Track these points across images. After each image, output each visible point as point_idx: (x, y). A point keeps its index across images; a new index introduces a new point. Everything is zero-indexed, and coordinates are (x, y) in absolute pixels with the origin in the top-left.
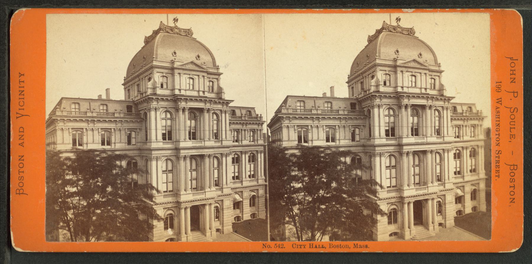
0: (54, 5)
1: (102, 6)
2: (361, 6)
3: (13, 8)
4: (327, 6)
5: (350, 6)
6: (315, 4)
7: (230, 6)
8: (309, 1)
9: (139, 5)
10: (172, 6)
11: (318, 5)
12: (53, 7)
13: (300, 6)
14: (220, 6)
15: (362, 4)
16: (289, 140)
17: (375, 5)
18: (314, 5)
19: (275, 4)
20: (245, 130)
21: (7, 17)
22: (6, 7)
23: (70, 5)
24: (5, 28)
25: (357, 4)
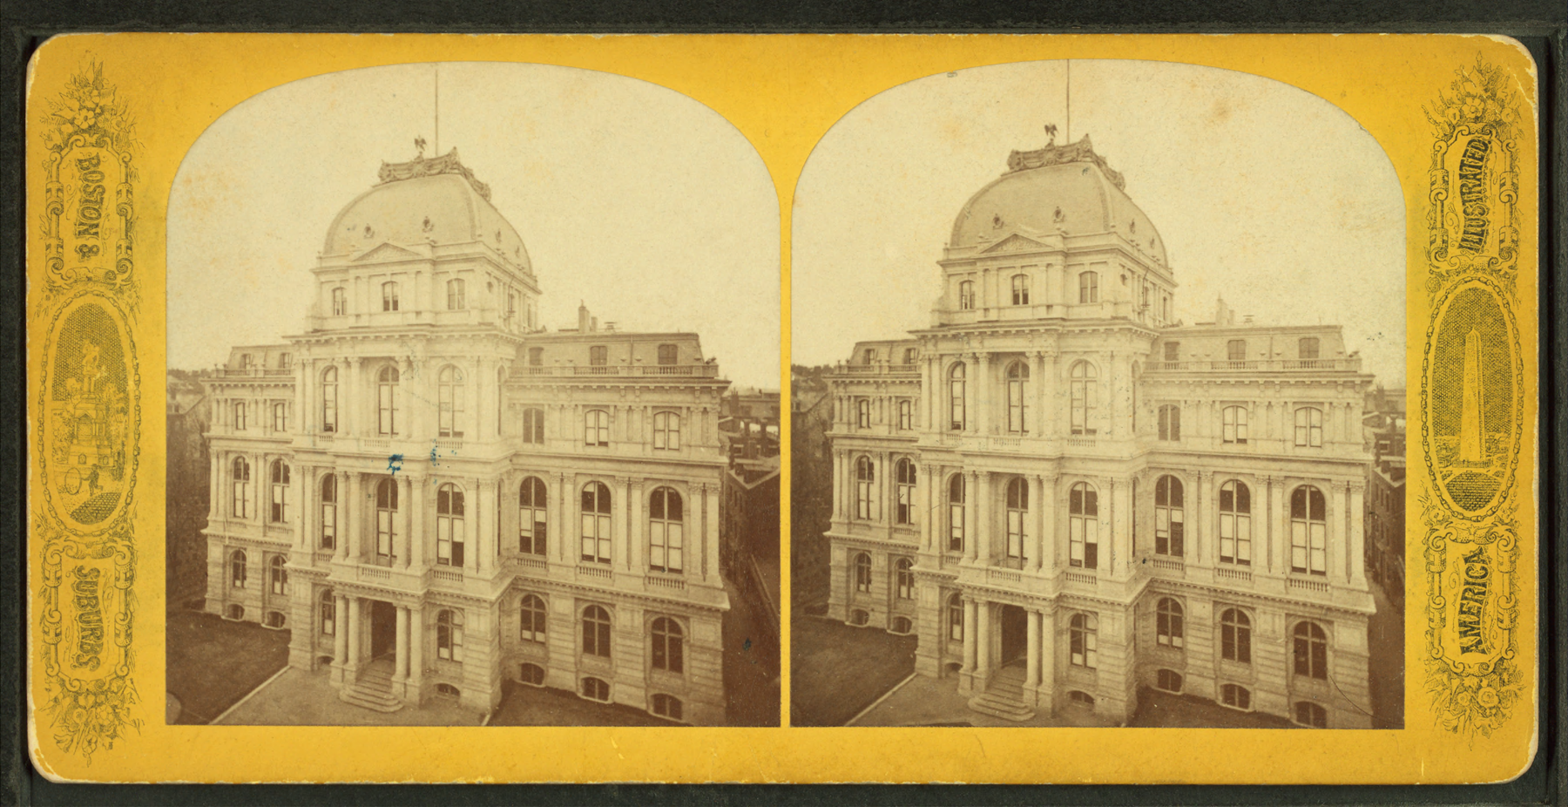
0: (152, 23)
1: (292, 27)
2: (1035, 24)
3: (35, 33)
4: (936, 27)
5: (1005, 27)
6: (905, 19)
7: (657, 26)
8: (886, 11)
9: (397, 24)
10: (491, 25)
11: (911, 23)
12: (150, 30)
13: (860, 24)
14: (631, 24)
15: (1040, 21)
16: (1199, 435)
17: (1076, 23)
18: (901, 23)
19: (787, 22)
20: (841, 399)
21: (19, 57)
22: (16, 29)
23: (200, 23)
24: (15, 90)
25: (1024, 20)
